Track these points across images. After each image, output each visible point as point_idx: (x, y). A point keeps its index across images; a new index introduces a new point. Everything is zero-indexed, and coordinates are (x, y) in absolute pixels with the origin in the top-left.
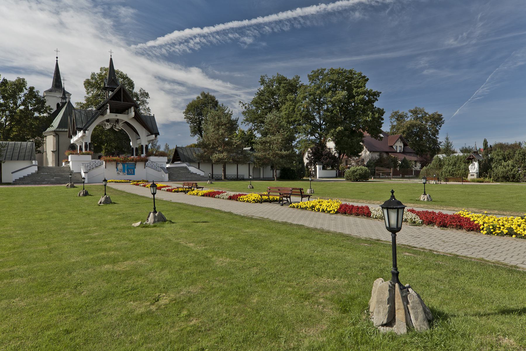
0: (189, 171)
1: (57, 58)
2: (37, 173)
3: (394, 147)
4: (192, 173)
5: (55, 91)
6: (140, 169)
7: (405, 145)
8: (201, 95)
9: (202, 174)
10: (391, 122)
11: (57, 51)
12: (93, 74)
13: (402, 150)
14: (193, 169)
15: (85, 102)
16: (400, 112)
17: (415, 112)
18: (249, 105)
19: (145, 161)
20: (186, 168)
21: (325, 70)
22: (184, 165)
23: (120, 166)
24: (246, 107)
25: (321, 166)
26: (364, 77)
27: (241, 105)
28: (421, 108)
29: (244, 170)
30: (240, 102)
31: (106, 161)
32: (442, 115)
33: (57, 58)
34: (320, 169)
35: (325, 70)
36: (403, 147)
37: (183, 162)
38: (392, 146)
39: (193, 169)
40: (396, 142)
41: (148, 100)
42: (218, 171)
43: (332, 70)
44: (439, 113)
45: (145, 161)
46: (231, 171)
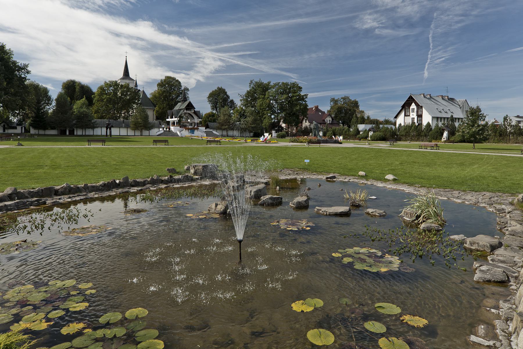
1: (126, 57)
3: (325, 120)
4: (214, 134)
6: (196, 131)
7: (332, 119)
8: (217, 88)
9: (218, 134)
10: (331, 105)
11: (126, 53)
14: (215, 132)
16: (336, 99)
17: (344, 99)
18: (244, 96)
20: (212, 132)
21: (280, 83)
22: (211, 130)
23: (190, 131)
24: (242, 97)
26: (300, 87)
27: (240, 96)
29: (236, 133)
31: (185, 129)
33: (126, 57)
34: (274, 133)
35: (280, 83)
36: (331, 120)
37: (211, 129)
38: (324, 120)
39: (215, 132)
41: (188, 92)
42: (225, 133)
43: (283, 83)
46: (230, 133)
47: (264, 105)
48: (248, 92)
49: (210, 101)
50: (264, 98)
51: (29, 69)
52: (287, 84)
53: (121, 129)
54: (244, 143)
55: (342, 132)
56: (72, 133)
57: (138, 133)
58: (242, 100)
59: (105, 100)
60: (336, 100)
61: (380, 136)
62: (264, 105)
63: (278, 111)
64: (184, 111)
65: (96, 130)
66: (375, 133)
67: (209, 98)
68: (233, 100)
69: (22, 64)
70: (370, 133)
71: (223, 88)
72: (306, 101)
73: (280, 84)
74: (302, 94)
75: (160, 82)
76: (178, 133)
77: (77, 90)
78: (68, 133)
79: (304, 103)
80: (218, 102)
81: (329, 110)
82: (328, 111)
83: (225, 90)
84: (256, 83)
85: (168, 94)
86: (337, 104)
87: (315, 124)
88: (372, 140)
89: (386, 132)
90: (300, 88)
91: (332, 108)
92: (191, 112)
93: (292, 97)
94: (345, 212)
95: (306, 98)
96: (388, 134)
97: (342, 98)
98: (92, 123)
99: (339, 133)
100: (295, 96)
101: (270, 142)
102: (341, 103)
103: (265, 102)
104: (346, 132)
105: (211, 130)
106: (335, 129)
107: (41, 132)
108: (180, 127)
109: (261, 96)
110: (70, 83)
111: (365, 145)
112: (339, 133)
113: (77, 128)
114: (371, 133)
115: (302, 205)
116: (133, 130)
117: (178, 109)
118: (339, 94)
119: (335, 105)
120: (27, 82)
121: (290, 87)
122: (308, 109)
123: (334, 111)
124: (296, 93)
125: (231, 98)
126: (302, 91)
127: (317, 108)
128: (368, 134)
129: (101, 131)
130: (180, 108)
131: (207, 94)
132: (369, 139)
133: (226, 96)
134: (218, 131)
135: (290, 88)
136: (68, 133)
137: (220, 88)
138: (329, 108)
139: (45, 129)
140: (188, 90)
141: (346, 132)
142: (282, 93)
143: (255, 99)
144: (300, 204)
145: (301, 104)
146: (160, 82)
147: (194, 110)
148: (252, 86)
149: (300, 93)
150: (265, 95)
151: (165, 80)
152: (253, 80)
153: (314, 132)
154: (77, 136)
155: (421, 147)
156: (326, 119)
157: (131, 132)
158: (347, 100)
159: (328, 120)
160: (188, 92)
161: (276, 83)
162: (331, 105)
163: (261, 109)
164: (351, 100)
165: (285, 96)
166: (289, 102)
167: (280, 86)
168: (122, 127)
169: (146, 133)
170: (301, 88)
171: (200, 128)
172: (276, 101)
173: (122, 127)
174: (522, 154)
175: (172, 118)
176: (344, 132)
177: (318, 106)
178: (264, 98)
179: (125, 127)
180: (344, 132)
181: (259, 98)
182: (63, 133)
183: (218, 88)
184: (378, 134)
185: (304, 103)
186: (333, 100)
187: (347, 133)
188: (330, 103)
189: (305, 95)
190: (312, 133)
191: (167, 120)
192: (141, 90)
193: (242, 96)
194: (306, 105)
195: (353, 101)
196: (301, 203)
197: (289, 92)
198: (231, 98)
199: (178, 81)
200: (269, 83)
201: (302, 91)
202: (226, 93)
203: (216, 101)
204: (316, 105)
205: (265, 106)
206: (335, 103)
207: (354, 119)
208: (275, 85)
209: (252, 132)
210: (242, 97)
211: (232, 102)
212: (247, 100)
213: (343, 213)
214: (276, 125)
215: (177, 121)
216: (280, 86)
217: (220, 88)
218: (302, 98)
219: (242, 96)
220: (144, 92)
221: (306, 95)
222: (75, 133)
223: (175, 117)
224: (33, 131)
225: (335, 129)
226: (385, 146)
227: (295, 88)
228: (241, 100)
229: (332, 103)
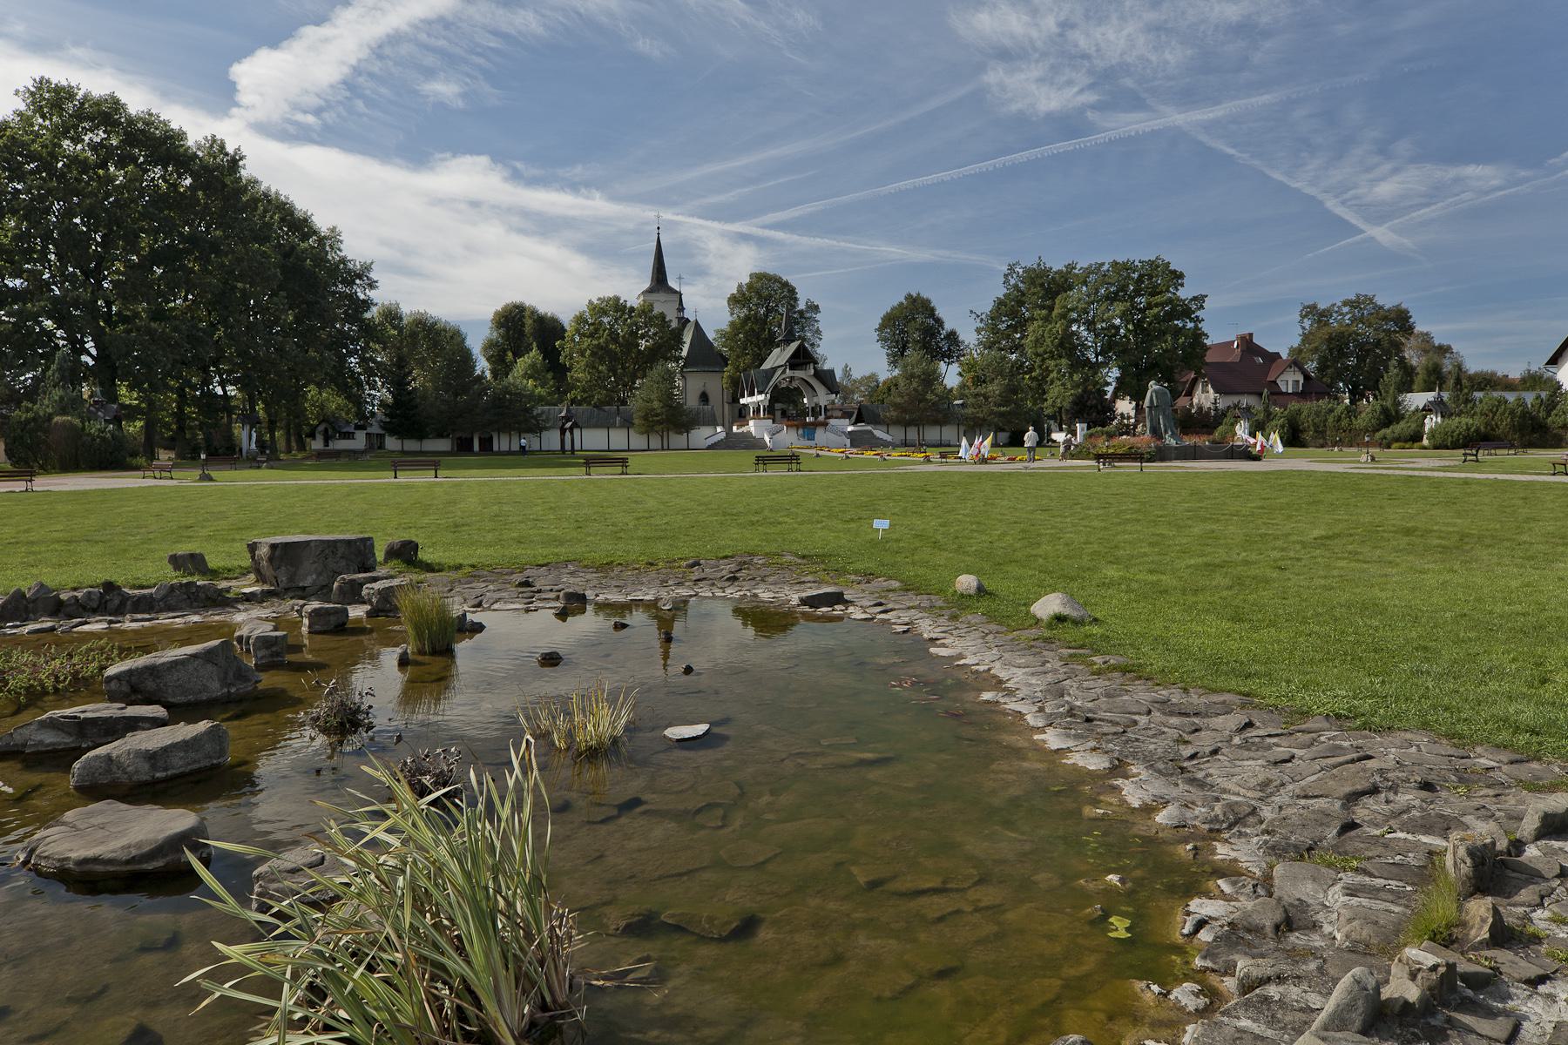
0: (874, 436)
2: (726, 438)
5: (658, 291)
6: (819, 433)
8: (906, 299)
9: (888, 438)
10: (1303, 328)
12: (740, 286)
13: (1301, 388)
15: (728, 330)
16: (1322, 306)
17: (1353, 304)
18: (987, 315)
19: (825, 424)
20: (870, 431)
21: (1103, 264)
22: (869, 428)
24: (982, 320)
25: (1085, 425)
26: (1175, 271)
27: (974, 316)
28: (1370, 294)
30: (971, 312)
32: (1410, 309)
34: (1083, 430)
35: (1103, 264)
36: (1302, 382)
37: (868, 423)
38: (1275, 382)
40: (1282, 373)
41: (818, 317)
42: (912, 434)
43: (1115, 264)
44: (1404, 306)
45: (825, 424)
47: (1048, 341)
48: (1000, 303)
49: (882, 339)
50: (1047, 319)
51: (373, 275)
52: (1127, 267)
53: (613, 433)
54: (921, 463)
55: (1326, 420)
56: (487, 446)
57: (655, 441)
58: (983, 329)
59: (588, 352)
60: (1324, 310)
61: (1468, 429)
62: (1048, 341)
63: (1097, 357)
64: (784, 372)
65: (545, 434)
66: (1446, 421)
67: (881, 329)
68: (955, 333)
69: (357, 264)
70: (1427, 421)
71: (925, 295)
72: (1198, 320)
73: (1105, 268)
74: (1184, 293)
75: (735, 292)
76: (767, 439)
77: (527, 329)
78: (476, 447)
79: (1190, 325)
80: (907, 342)
81: (1296, 345)
82: (1292, 351)
83: (929, 301)
84: (1026, 270)
85: (756, 327)
86: (1327, 324)
87: (1155, 391)
88: (1436, 448)
89: (1495, 414)
90: (1177, 277)
91: (1306, 338)
92: (807, 374)
93: (1145, 309)
94: (110, 862)
95: (1199, 309)
96: (1504, 424)
97: (1345, 303)
98: (533, 417)
99: (1314, 424)
100: (1157, 305)
101: (1014, 459)
102: (1341, 320)
103: (1051, 330)
104: (1339, 419)
105: (869, 428)
106: (1299, 412)
107: (411, 445)
108: (774, 422)
109: (1037, 312)
110: (511, 312)
111: (1359, 462)
112: (1314, 424)
113: (499, 431)
114: (1432, 422)
115: (119, 774)
116: (642, 433)
117: (769, 367)
118: (1333, 292)
119: (1318, 328)
120: (373, 313)
121: (1141, 276)
122: (1205, 348)
123: (1316, 350)
124: (1161, 293)
125: (948, 326)
126: (1182, 285)
127: (1247, 343)
128: (1423, 424)
129: (552, 439)
130: (776, 365)
131: (877, 322)
132: (1425, 442)
133: (934, 319)
134: (893, 430)
135: (1140, 280)
136: (476, 447)
137: (915, 295)
138: (1296, 342)
139: (421, 436)
140: (816, 309)
141: (1339, 419)
142: (1111, 298)
143: (1021, 325)
144: (109, 771)
145: (1178, 332)
146: (735, 292)
147: (814, 368)
148: (1012, 282)
149: (1178, 293)
150: (1051, 309)
151: (750, 286)
152: (1018, 263)
153: (1151, 421)
154: (500, 453)
155: (1560, 468)
156: (1283, 377)
157: (638, 441)
158: (1365, 308)
159: (1289, 381)
160: (818, 317)
161: (1091, 266)
162: (1303, 328)
163: (1037, 355)
164: (1381, 308)
165: (1119, 307)
166: (1138, 325)
167: (1105, 275)
168: (615, 427)
169: (678, 440)
170: (1181, 276)
171: (832, 422)
172: (1090, 325)
173: (613, 426)
174: (1554, 474)
175: (752, 394)
176: (1331, 419)
177: (1251, 335)
178: (1047, 319)
179: (622, 426)
180: (1331, 419)
181: (1032, 319)
182: (464, 447)
183: (909, 297)
184: (1462, 422)
185: (1190, 325)
186: (1310, 311)
187: (1344, 423)
188: (1301, 321)
189: (1195, 299)
190: (1145, 426)
191: (742, 401)
192: (692, 319)
193: (983, 316)
194: (1198, 335)
195: (1389, 310)
196: (120, 766)
197: (1138, 293)
198: (948, 326)
199: (786, 284)
200: (1071, 267)
201: (1182, 285)
202: (933, 310)
203: (902, 338)
204: (1246, 331)
205: (1052, 342)
206: (1319, 321)
207: (1393, 373)
208: (1088, 271)
209: (1003, 430)
210: (982, 320)
211: (952, 336)
212: (994, 330)
213: (100, 868)
214: (1089, 403)
215: (767, 404)
216: (1105, 275)
217: (915, 295)
218: (1185, 311)
219: (983, 316)
220: (697, 323)
221: (1200, 300)
222: (495, 448)
223: (760, 393)
224: (392, 443)
225: (1299, 412)
226: (1437, 463)
227: (1158, 277)
228: (978, 331)
229: (1307, 323)
